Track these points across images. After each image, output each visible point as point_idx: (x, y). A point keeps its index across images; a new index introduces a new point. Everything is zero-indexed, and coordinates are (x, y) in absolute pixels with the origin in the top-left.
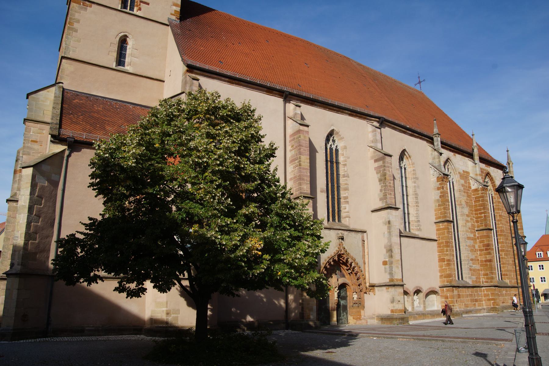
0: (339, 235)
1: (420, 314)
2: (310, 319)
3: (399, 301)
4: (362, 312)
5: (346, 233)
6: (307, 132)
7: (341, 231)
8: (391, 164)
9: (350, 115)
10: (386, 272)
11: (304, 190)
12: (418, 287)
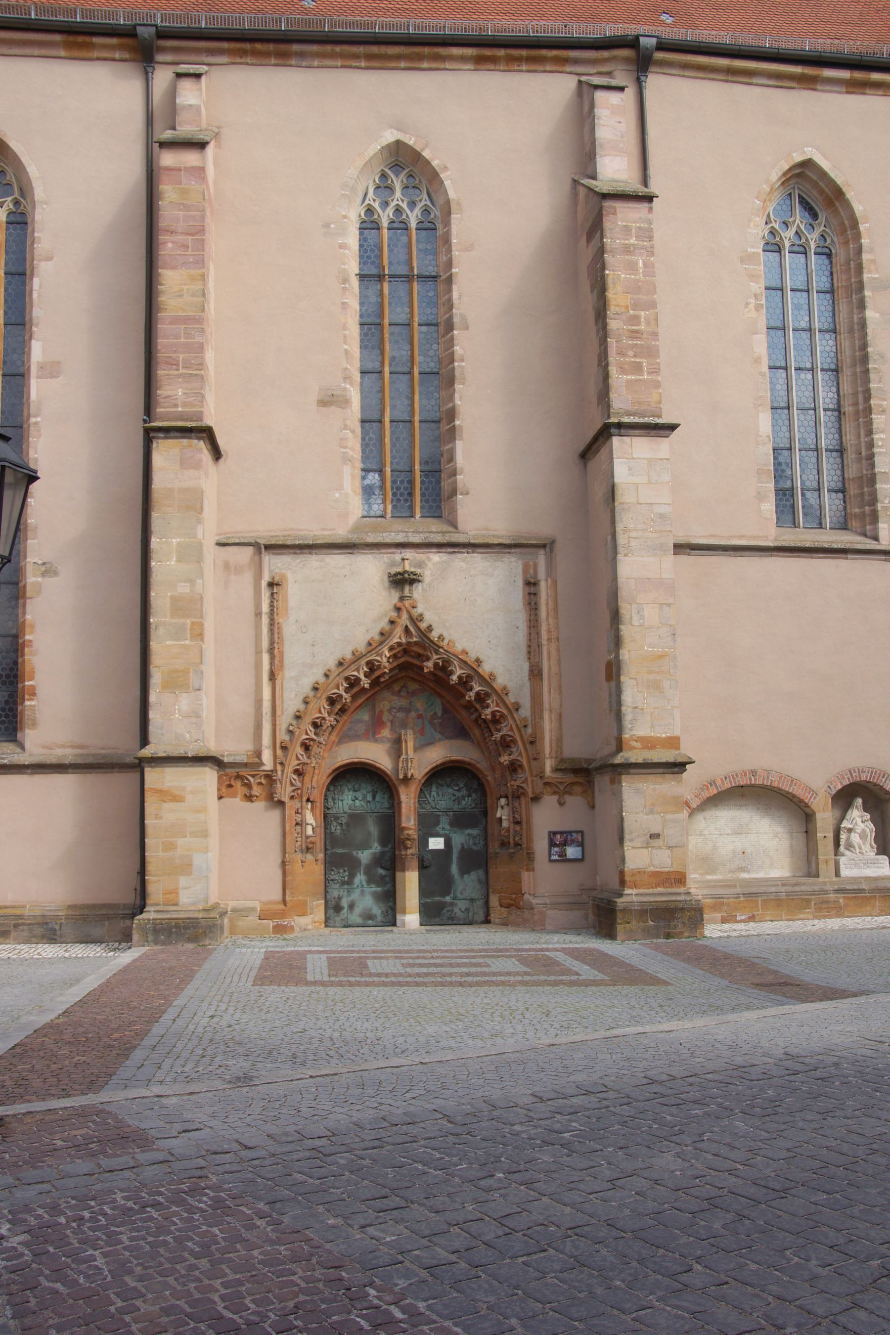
0: (393, 571)
1: (861, 891)
2: (176, 904)
3: (655, 836)
4: (525, 876)
5: (436, 558)
6: (200, 171)
7: (408, 554)
8: (647, 234)
9: (480, 61)
10: (611, 711)
11: (176, 406)
12: (861, 771)
